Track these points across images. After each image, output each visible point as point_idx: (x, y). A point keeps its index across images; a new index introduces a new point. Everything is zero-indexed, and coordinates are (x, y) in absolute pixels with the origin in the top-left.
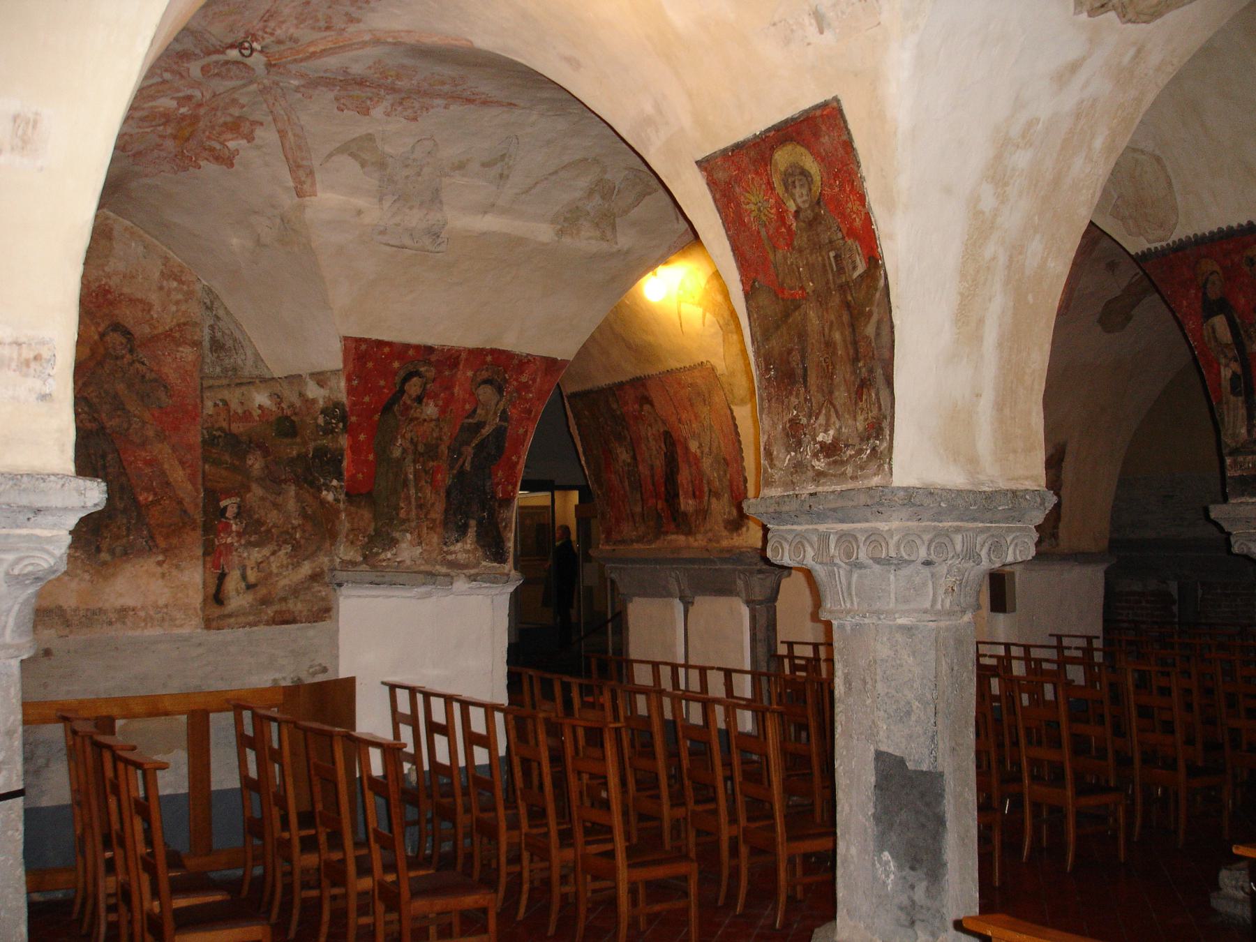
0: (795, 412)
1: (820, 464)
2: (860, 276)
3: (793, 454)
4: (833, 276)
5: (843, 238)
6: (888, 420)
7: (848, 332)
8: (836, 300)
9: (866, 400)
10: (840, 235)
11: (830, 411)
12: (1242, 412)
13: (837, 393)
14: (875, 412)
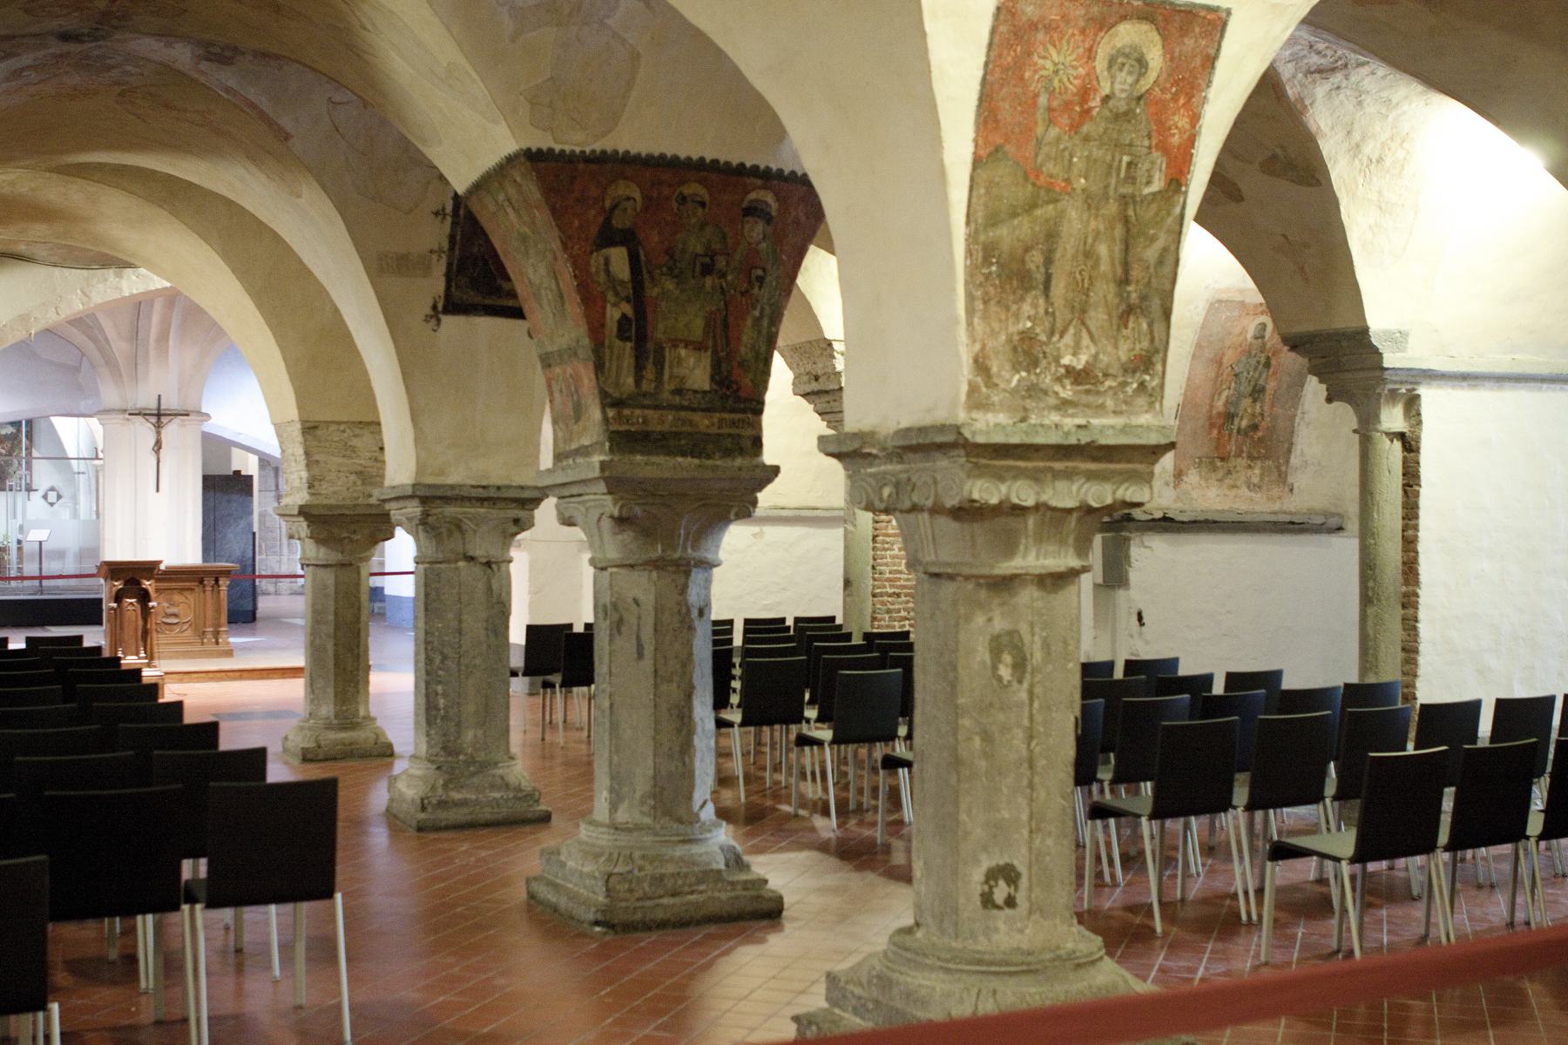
0: (1029, 324)
1: (1067, 392)
2: (1154, 194)
3: (1024, 374)
4: (1117, 182)
5: (1150, 148)
6: (1161, 355)
7: (1118, 248)
8: (1112, 208)
9: (1133, 329)
10: (1146, 143)
11: (1081, 330)
12: (628, 361)
13: (1092, 313)
14: (1145, 344)
